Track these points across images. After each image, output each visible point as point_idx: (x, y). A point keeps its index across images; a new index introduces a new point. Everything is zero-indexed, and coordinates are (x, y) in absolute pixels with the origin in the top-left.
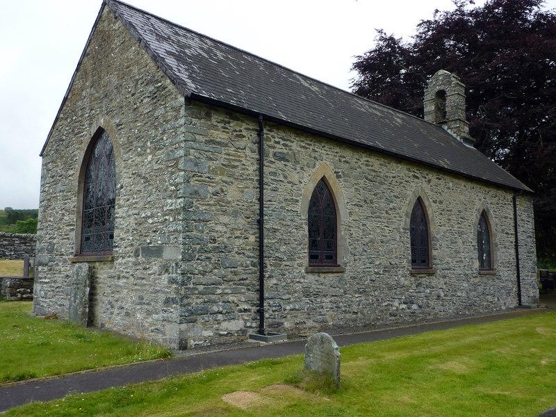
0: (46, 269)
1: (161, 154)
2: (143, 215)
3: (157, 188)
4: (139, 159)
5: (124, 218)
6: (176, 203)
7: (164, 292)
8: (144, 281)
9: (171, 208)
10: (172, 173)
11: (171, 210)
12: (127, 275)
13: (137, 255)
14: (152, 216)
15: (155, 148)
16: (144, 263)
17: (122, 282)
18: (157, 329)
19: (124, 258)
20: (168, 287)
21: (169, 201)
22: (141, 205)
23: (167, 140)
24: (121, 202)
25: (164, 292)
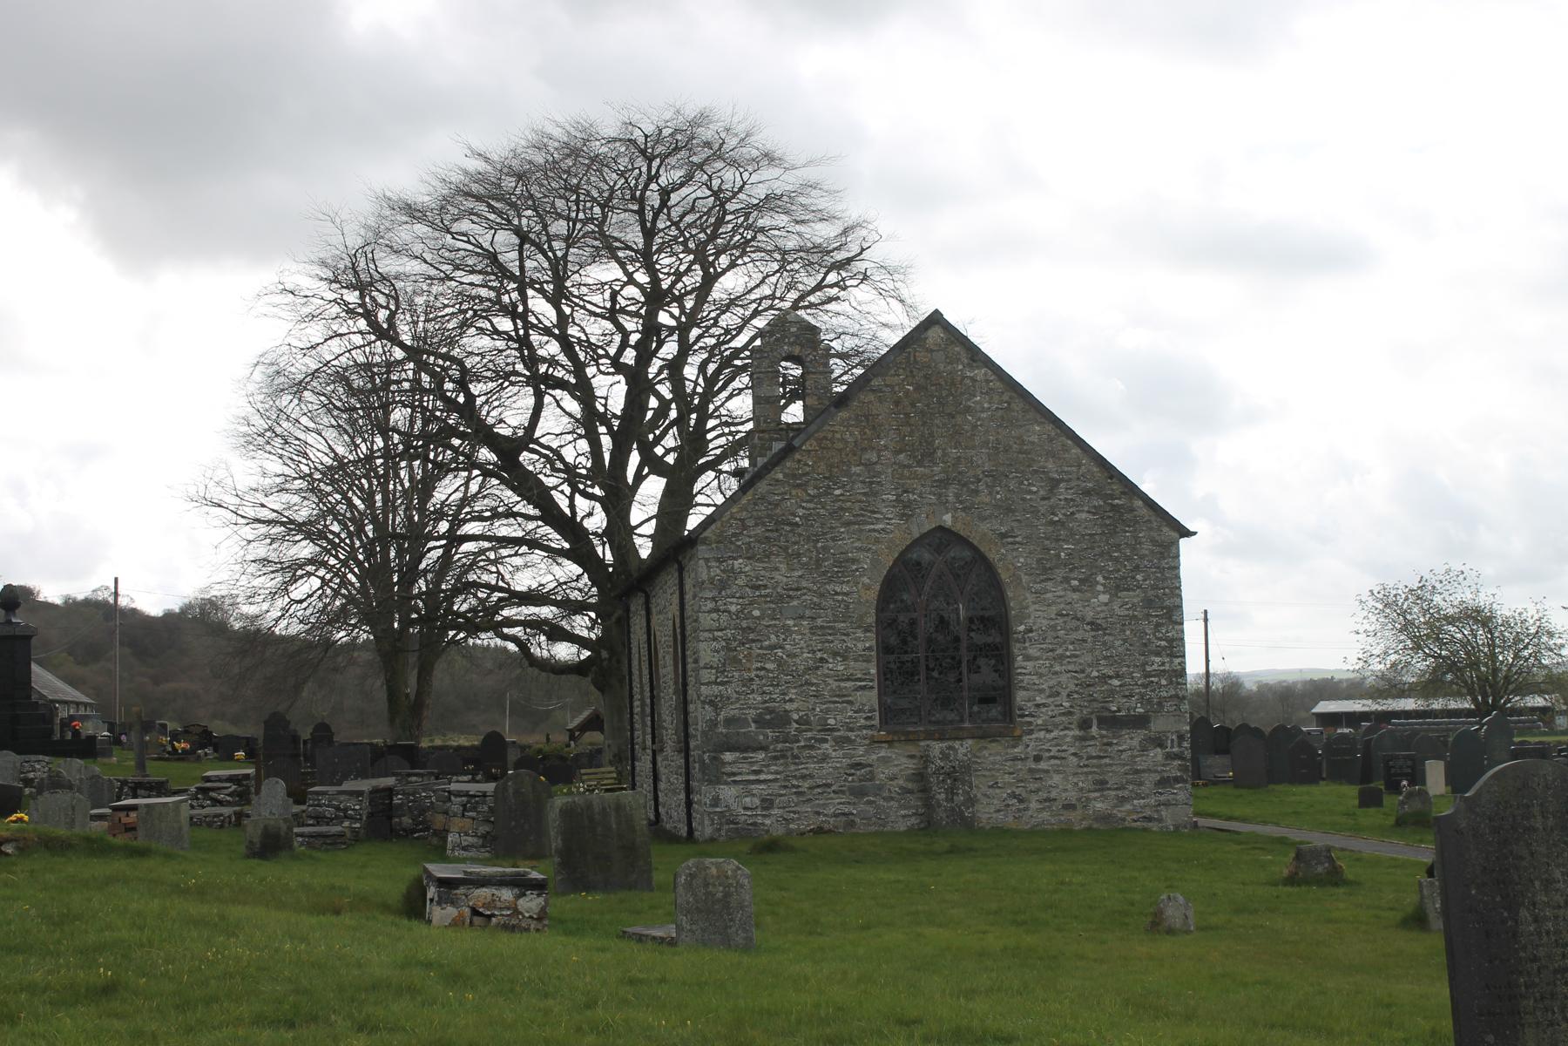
0: (761, 755)
1: (1135, 597)
2: (1095, 674)
3: (1125, 641)
4: (1076, 596)
5: (1041, 676)
6: (1171, 662)
7: (1156, 771)
8: (1107, 761)
9: (1162, 668)
10: (1158, 625)
11: (1164, 671)
12: (1063, 755)
13: (1085, 724)
14: (1117, 676)
15: (1118, 587)
16: (1103, 736)
17: (1043, 765)
18: (1145, 817)
19: (1049, 731)
20: (1164, 765)
21: (1158, 659)
22: (1088, 658)
23: (1145, 580)
24: (1033, 652)
25: (1156, 771)
